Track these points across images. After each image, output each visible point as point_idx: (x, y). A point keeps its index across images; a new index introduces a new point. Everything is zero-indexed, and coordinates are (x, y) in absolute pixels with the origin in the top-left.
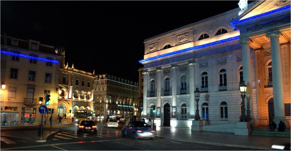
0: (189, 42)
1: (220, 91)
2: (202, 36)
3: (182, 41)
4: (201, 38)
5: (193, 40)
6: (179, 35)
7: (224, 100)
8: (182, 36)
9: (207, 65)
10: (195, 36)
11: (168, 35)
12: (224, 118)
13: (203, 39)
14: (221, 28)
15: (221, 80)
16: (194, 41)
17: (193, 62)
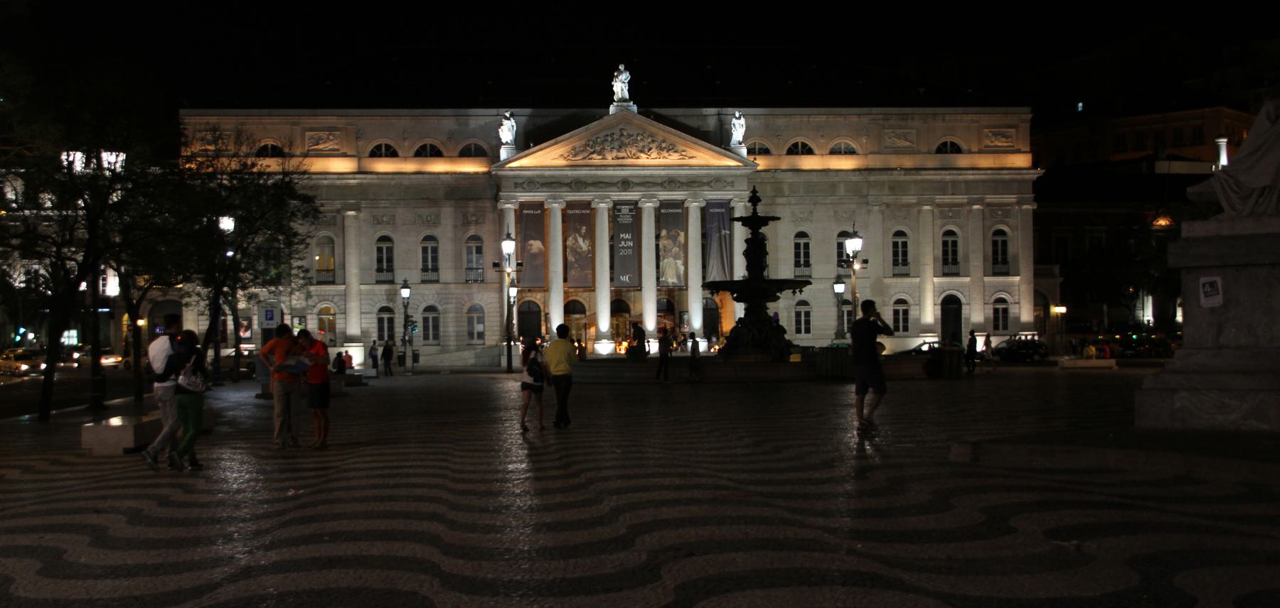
0: (345, 155)
1: (423, 282)
2: (378, 147)
3: (321, 147)
4: (376, 153)
5: (353, 153)
6: (311, 130)
7: (431, 303)
8: (321, 134)
9: (392, 222)
10: (360, 143)
11: (277, 120)
12: (431, 341)
13: (380, 156)
14: (428, 141)
15: (425, 260)
16: (358, 156)
17: (357, 209)
